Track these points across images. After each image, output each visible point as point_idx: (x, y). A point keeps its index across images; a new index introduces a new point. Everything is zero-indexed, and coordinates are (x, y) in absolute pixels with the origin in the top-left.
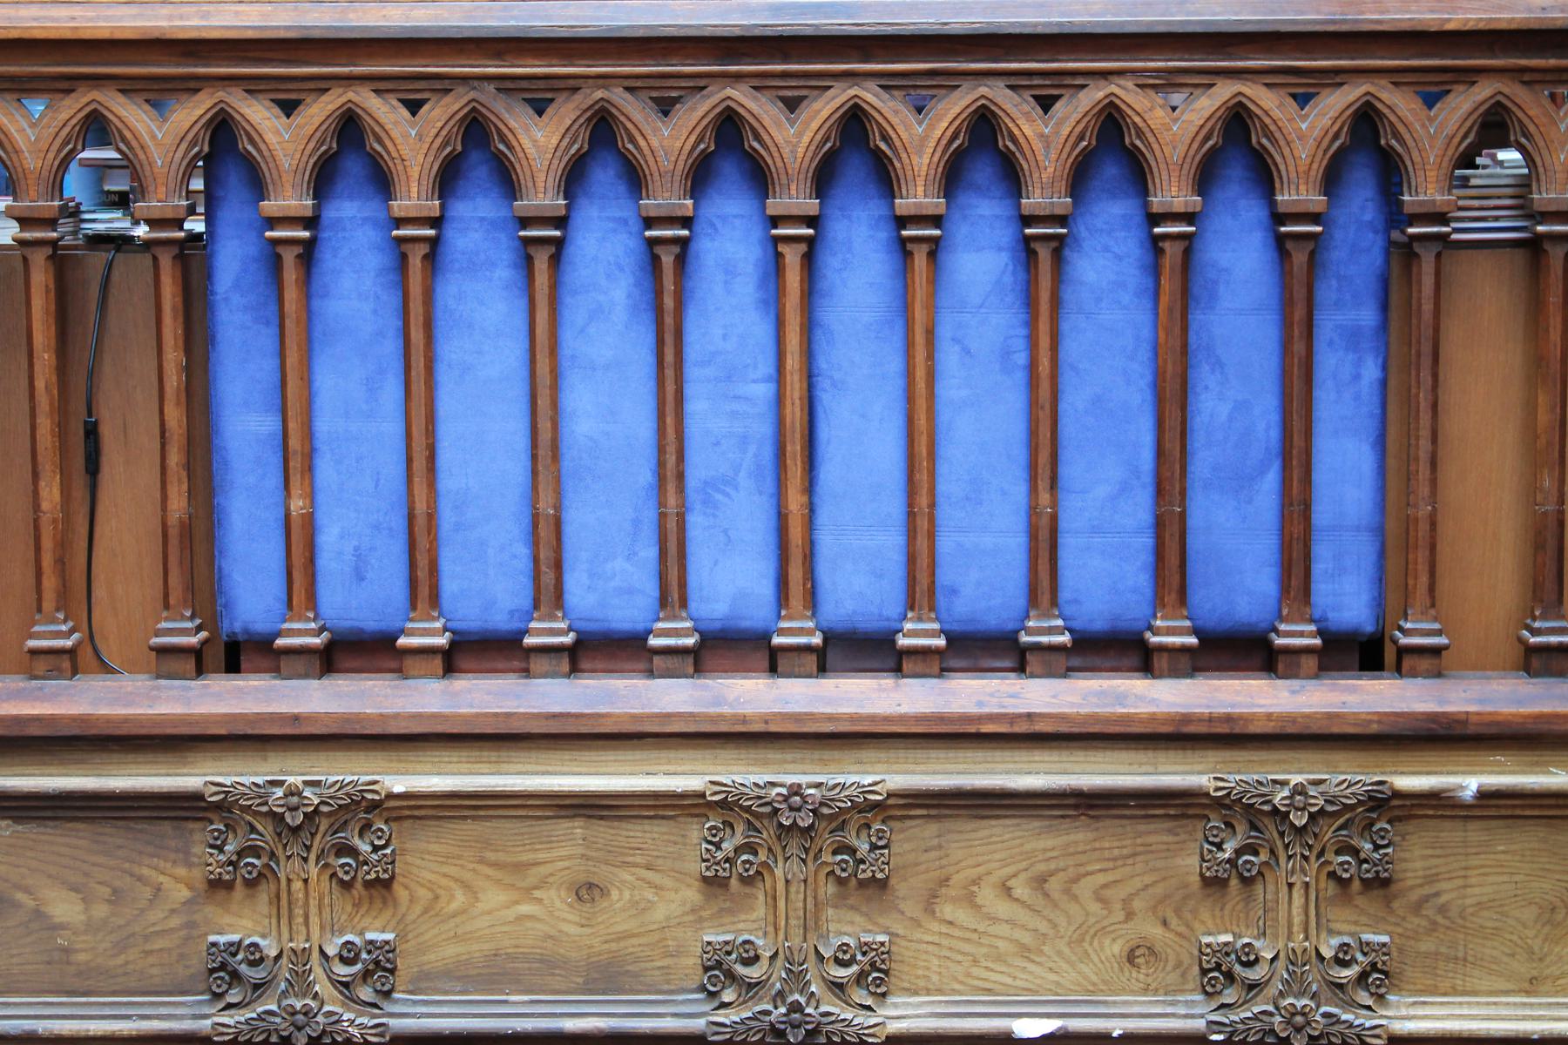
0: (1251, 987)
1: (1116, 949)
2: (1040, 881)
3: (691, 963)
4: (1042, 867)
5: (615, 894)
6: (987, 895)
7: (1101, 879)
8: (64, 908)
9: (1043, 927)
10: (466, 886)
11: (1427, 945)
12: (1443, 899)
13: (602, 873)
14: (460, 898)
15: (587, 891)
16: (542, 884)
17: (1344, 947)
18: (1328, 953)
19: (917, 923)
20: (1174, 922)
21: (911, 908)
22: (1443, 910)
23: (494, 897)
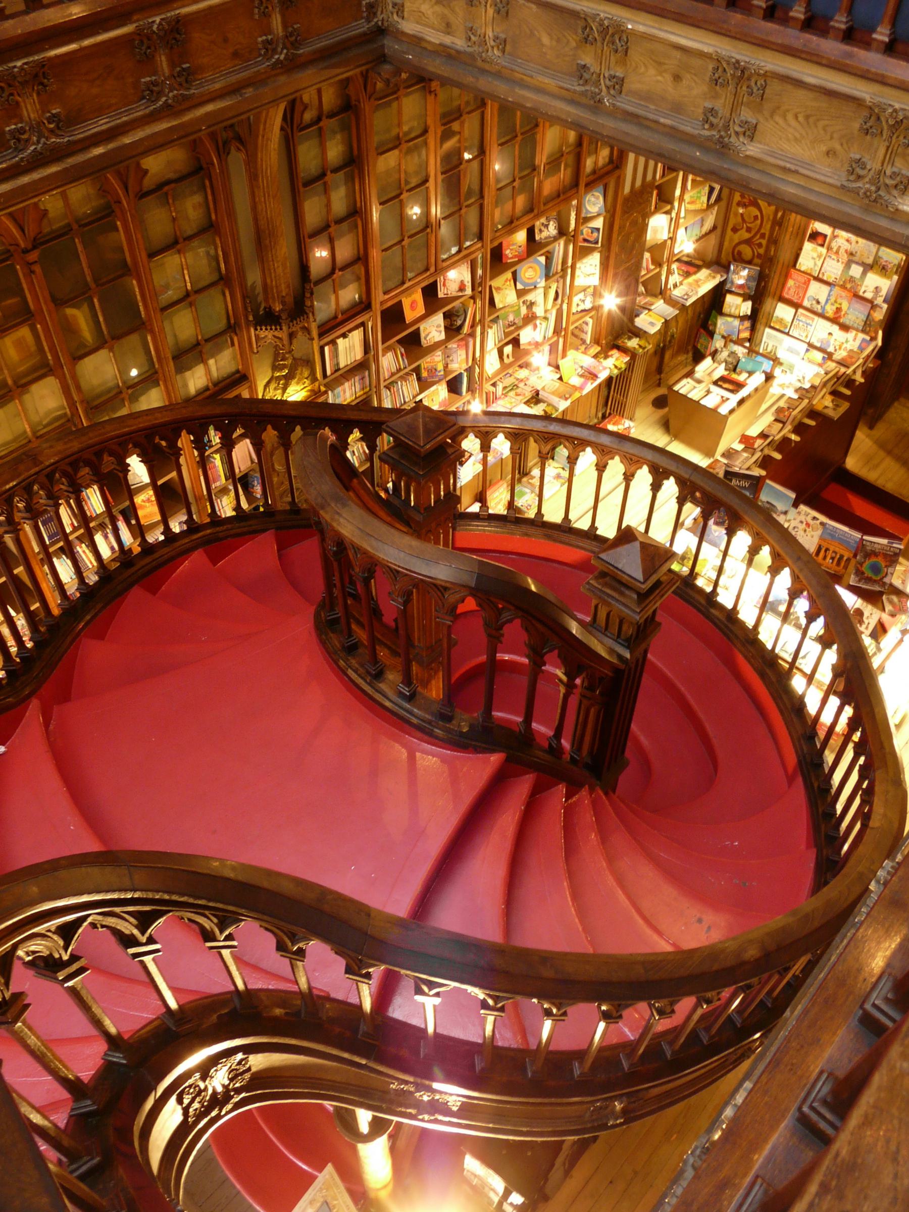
1: (824, 148)
2: (807, 117)
3: (700, 111)
5: (684, 82)
6: (790, 117)
7: (826, 122)
8: (546, 40)
9: (804, 133)
10: (646, 66)
14: (643, 69)
16: (665, 71)
18: (888, 172)
19: (767, 119)
20: (845, 146)
23: (652, 71)
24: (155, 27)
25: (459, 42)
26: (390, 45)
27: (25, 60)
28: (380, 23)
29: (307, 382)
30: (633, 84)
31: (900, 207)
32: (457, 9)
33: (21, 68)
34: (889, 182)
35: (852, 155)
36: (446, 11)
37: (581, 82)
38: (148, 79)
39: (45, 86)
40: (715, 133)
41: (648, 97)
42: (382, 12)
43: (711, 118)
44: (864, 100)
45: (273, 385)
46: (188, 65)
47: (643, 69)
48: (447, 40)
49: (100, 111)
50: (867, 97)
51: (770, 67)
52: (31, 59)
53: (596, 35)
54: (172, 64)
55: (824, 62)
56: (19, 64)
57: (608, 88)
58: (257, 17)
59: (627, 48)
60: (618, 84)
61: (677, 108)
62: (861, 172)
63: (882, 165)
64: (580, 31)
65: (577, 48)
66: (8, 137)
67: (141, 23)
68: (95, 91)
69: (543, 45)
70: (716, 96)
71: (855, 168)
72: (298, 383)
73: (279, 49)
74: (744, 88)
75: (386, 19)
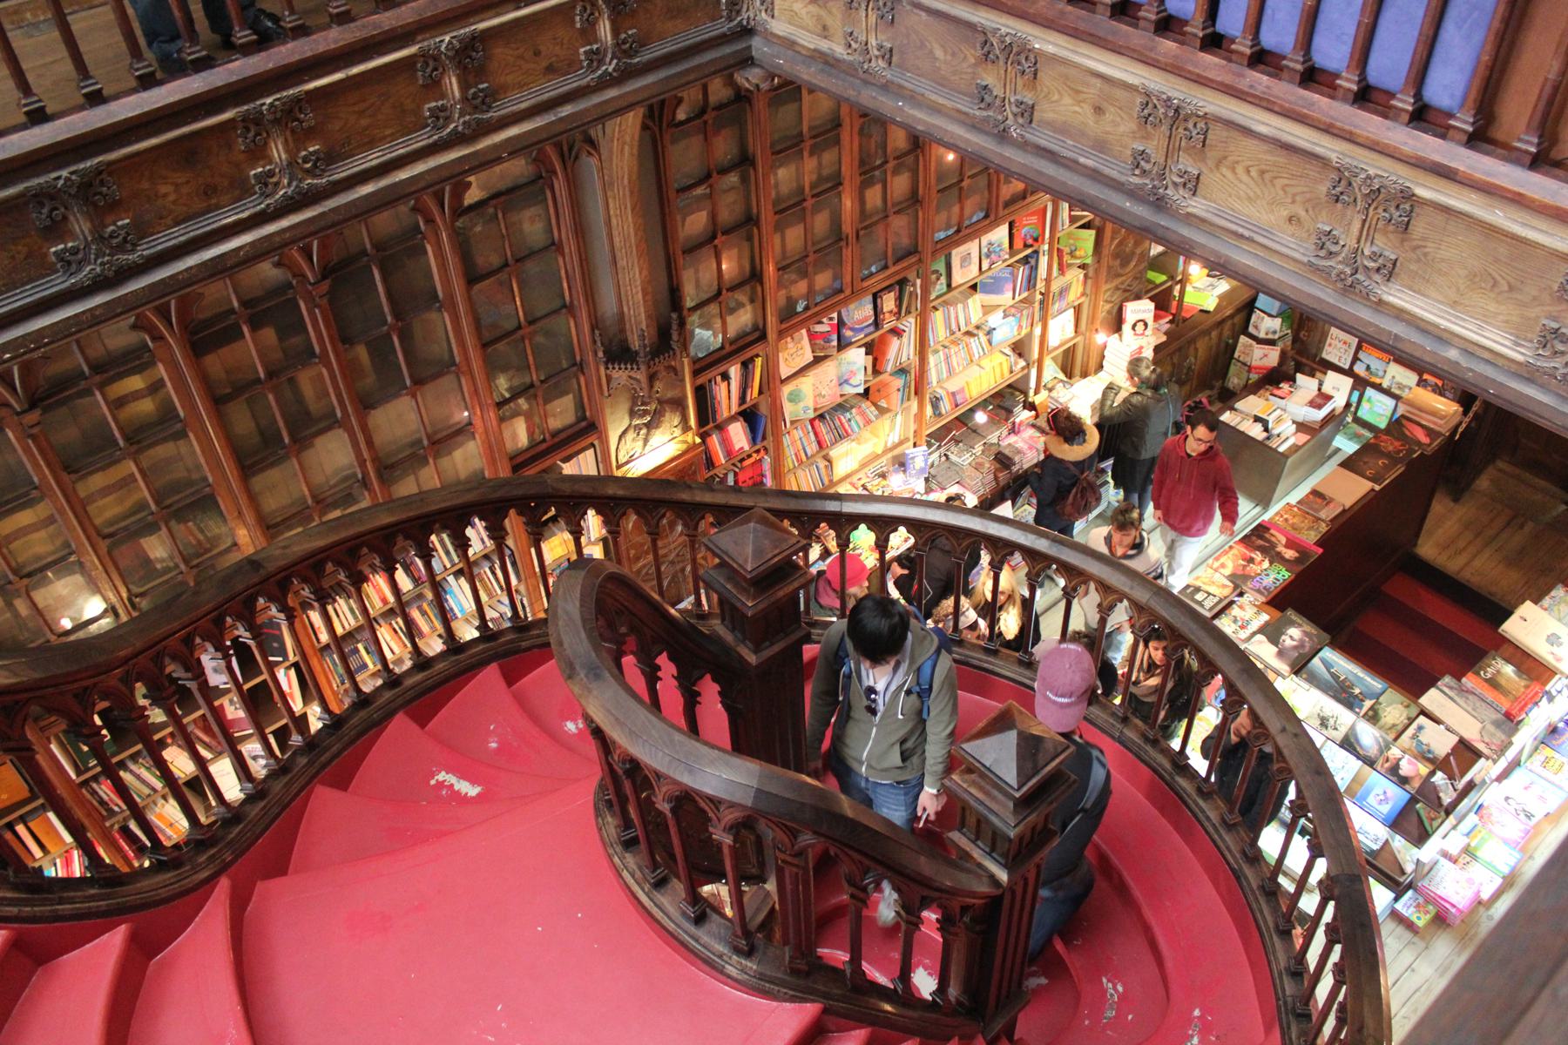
0: (1331, 253)
1: (1285, 213)
2: (1262, 172)
3: (1129, 153)
4: (1264, 167)
6: (1240, 170)
7: (1286, 182)
8: (939, 53)
9: (1259, 193)
11: (1413, 267)
12: (1427, 250)
13: (1105, 105)
14: (1056, 97)
16: (1084, 101)
18: (1367, 252)
20: (1311, 212)
21: (1211, 163)
22: (1425, 255)
23: (1067, 100)
24: (444, 46)
25: (839, 50)
26: (758, 46)
27: (278, 96)
28: (745, 23)
29: (678, 432)
30: (1044, 112)
31: (1386, 297)
32: (834, 10)
33: (271, 105)
34: (1372, 265)
35: (1320, 226)
36: (823, 13)
37: (982, 106)
38: (434, 104)
39: (302, 122)
40: (1147, 181)
41: (1063, 129)
42: (748, 10)
43: (1142, 163)
44: (1329, 160)
45: (631, 435)
46: (485, 85)
47: (1056, 97)
48: (824, 45)
49: (371, 144)
50: (1333, 157)
51: (1210, 109)
52: (285, 94)
53: (998, 52)
54: (464, 87)
55: (1276, 109)
56: (269, 101)
57: (1015, 115)
58: (578, 25)
59: (1036, 70)
60: (1027, 112)
61: (1101, 146)
62: (1334, 249)
63: (1358, 242)
64: (978, 45)
65: (975, 65)
66: (253, 182)
67: (426, 43)
68: (364, 122)
69: (936, 59)
70: (1147, 137)
71: (1325, 242)
72: (663, 433)
73: (608, 60)
74: (1181, 130)
75: (752, 16)
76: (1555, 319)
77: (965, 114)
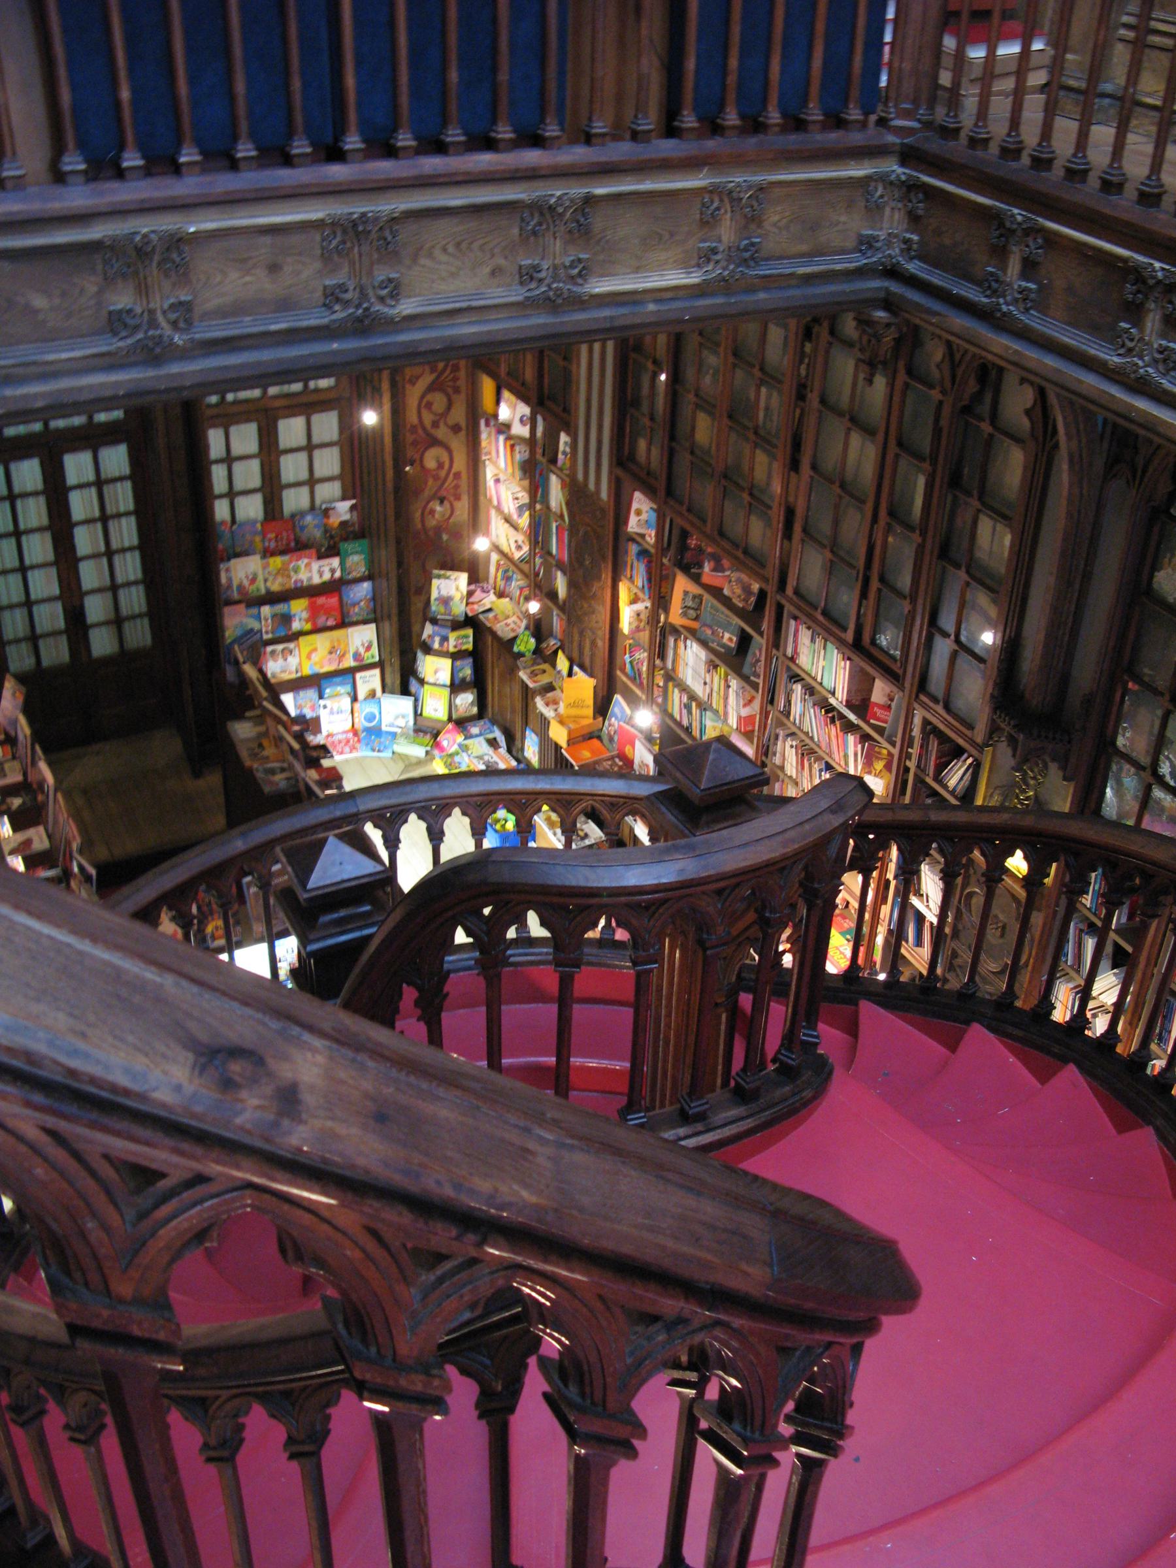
2: (458, 245)
3: (319, 294)
5: (285, 268)
6: (437, 252)
7: (482, 241)
8: (39, 302)
11: (601, 257)
15: (274, 268)
16: (254, 266)
17: (573, 261)
19: (410, 268)
22: (607, 242)
23: (234, 275)
30: (210, 300)
41: (237, 310)
47: (218, 279)
60: (184, 313)
61: (284, 305)
65: (100, 292)
69: (36, 312)
76: (704, 241)
77: (108, 354)
